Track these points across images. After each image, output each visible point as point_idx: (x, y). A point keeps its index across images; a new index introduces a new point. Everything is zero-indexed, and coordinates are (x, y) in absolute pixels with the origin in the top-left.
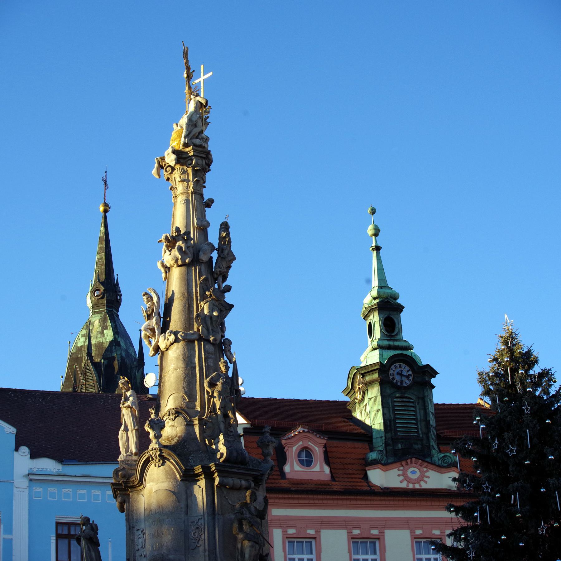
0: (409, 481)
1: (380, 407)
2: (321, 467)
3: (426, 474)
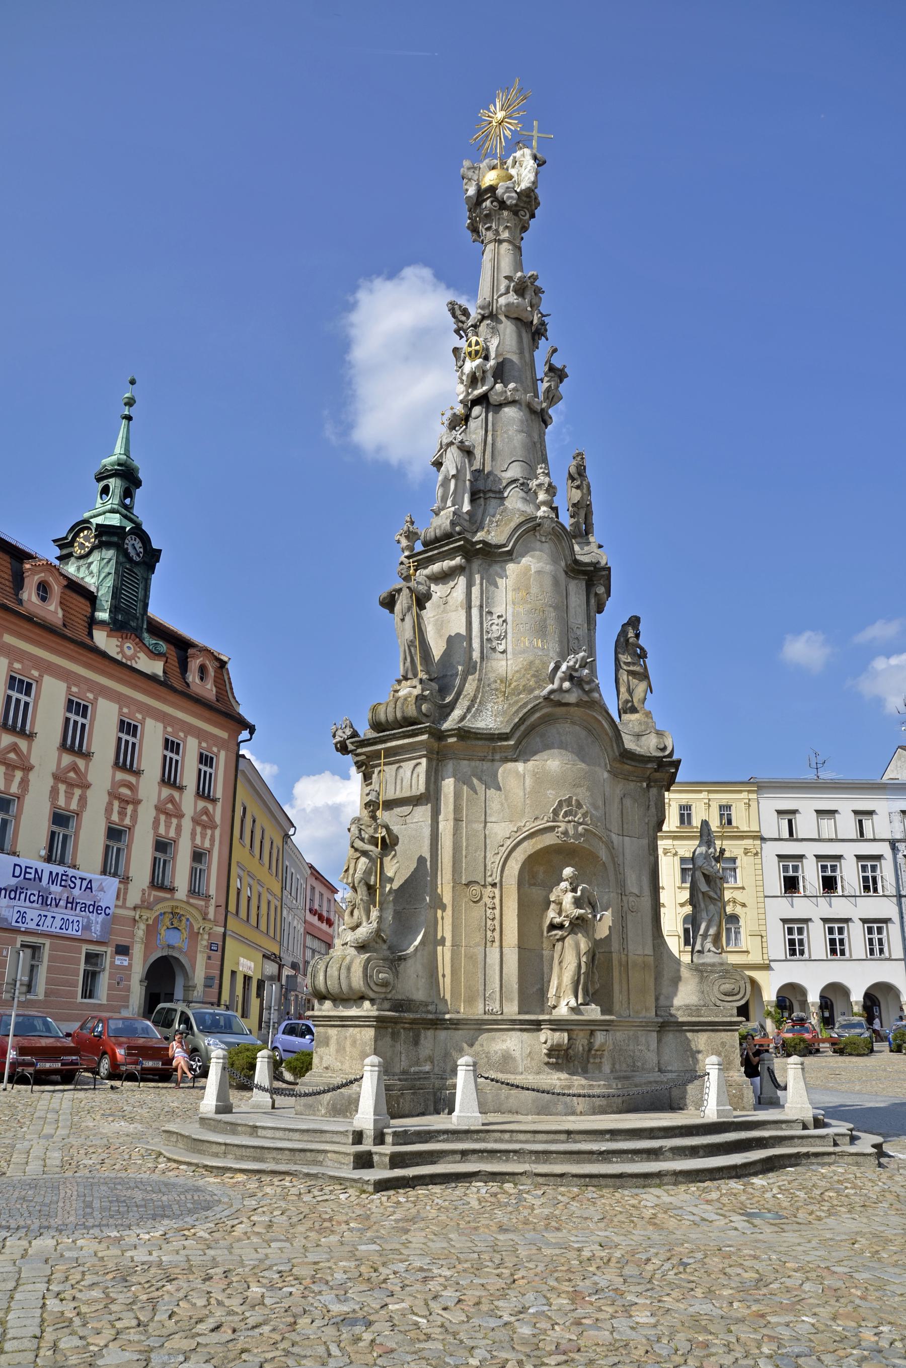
0: (124, 656)
1: (113, 571)
2: (56, 609)
3: (139, 655)
